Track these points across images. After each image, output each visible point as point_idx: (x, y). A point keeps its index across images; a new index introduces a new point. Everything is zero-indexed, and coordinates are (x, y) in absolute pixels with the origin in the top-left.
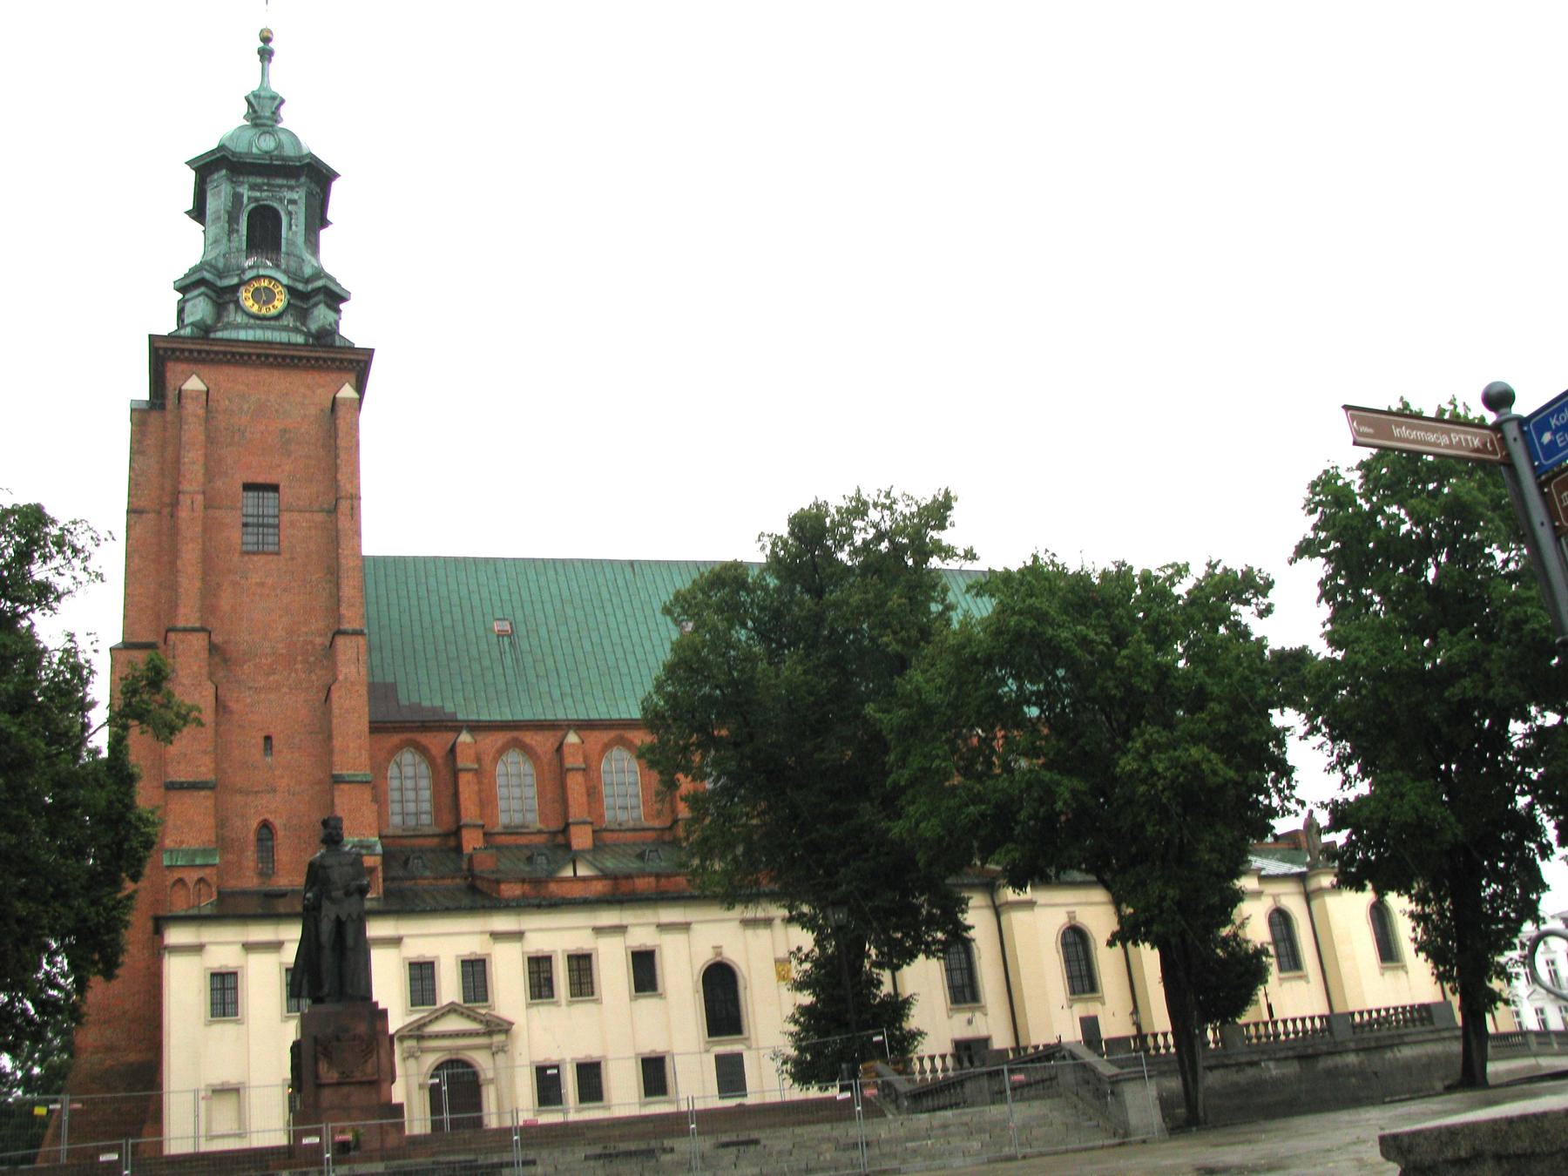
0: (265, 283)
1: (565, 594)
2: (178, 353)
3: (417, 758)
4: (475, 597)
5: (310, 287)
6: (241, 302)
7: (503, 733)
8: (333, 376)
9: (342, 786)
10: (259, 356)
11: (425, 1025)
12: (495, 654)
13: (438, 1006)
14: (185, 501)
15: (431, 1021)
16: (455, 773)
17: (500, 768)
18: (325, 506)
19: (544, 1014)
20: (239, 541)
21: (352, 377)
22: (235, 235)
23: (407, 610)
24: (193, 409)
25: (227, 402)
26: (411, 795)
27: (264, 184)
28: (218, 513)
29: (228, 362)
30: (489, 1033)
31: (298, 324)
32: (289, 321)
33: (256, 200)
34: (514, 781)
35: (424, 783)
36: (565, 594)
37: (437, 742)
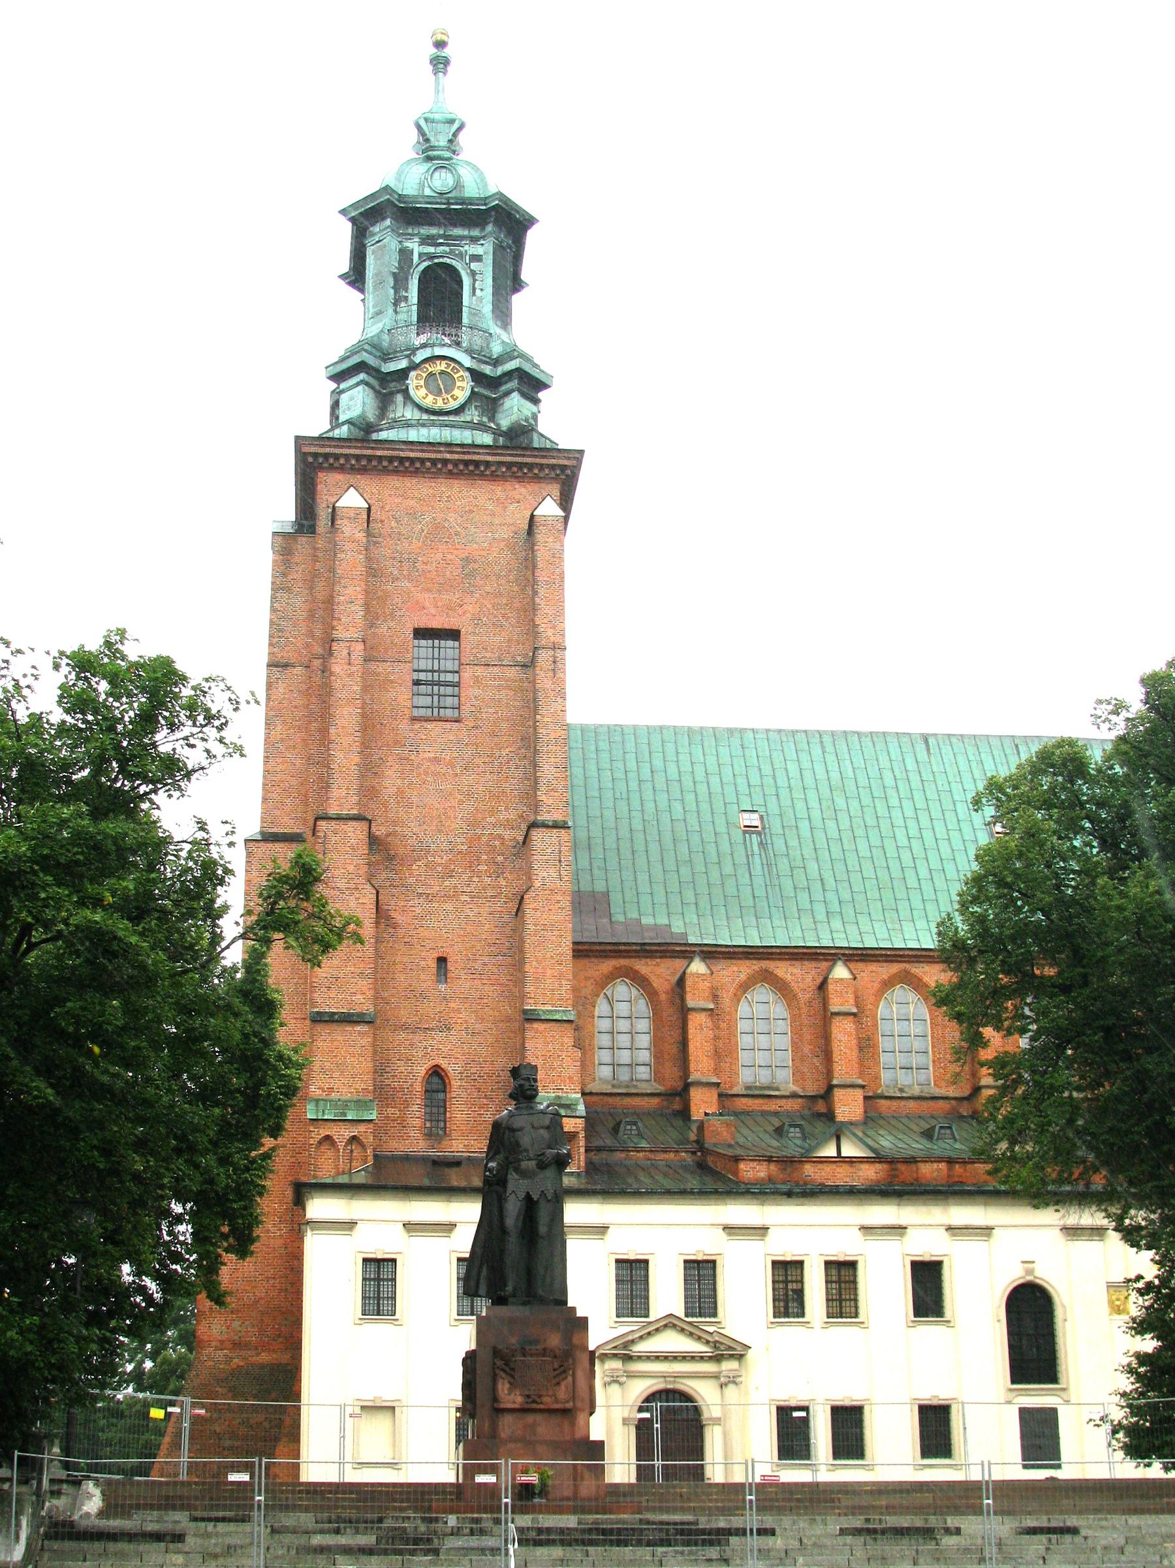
0: (441, 366)
1: (835, 776)
2: (331, 461)
3: (634, 992)
4: (715, 781)
5: (500, 371)
6: (412, 392)
7: (748, 962)
8: (533, 487)
9: (536, 1025)
10: (434, 462)
11: (633, 1342)
12: (740, 858)
13: (652, 1318)
14: (340, 650)
15: (641, 1337)
16: (684, 1012)
17: (743, 1009)
18: (519, 659)
19: (790, 1333)
20: (409, 704)
21: (555, 489)
22: (403, 304)
23: (624, 796)
24: (351, 531)
25: (393, 524)
26: (624, 1040)
27: (440, 236)
28: (381, 668)
29: (396, 472)
30: (717, 1359)
31: (485, 419)
32: (472, 415)
33: (431, 257)
34: (762, 1026)
35: (643, 1025)
36: (835, 776)
37: (661, 973)
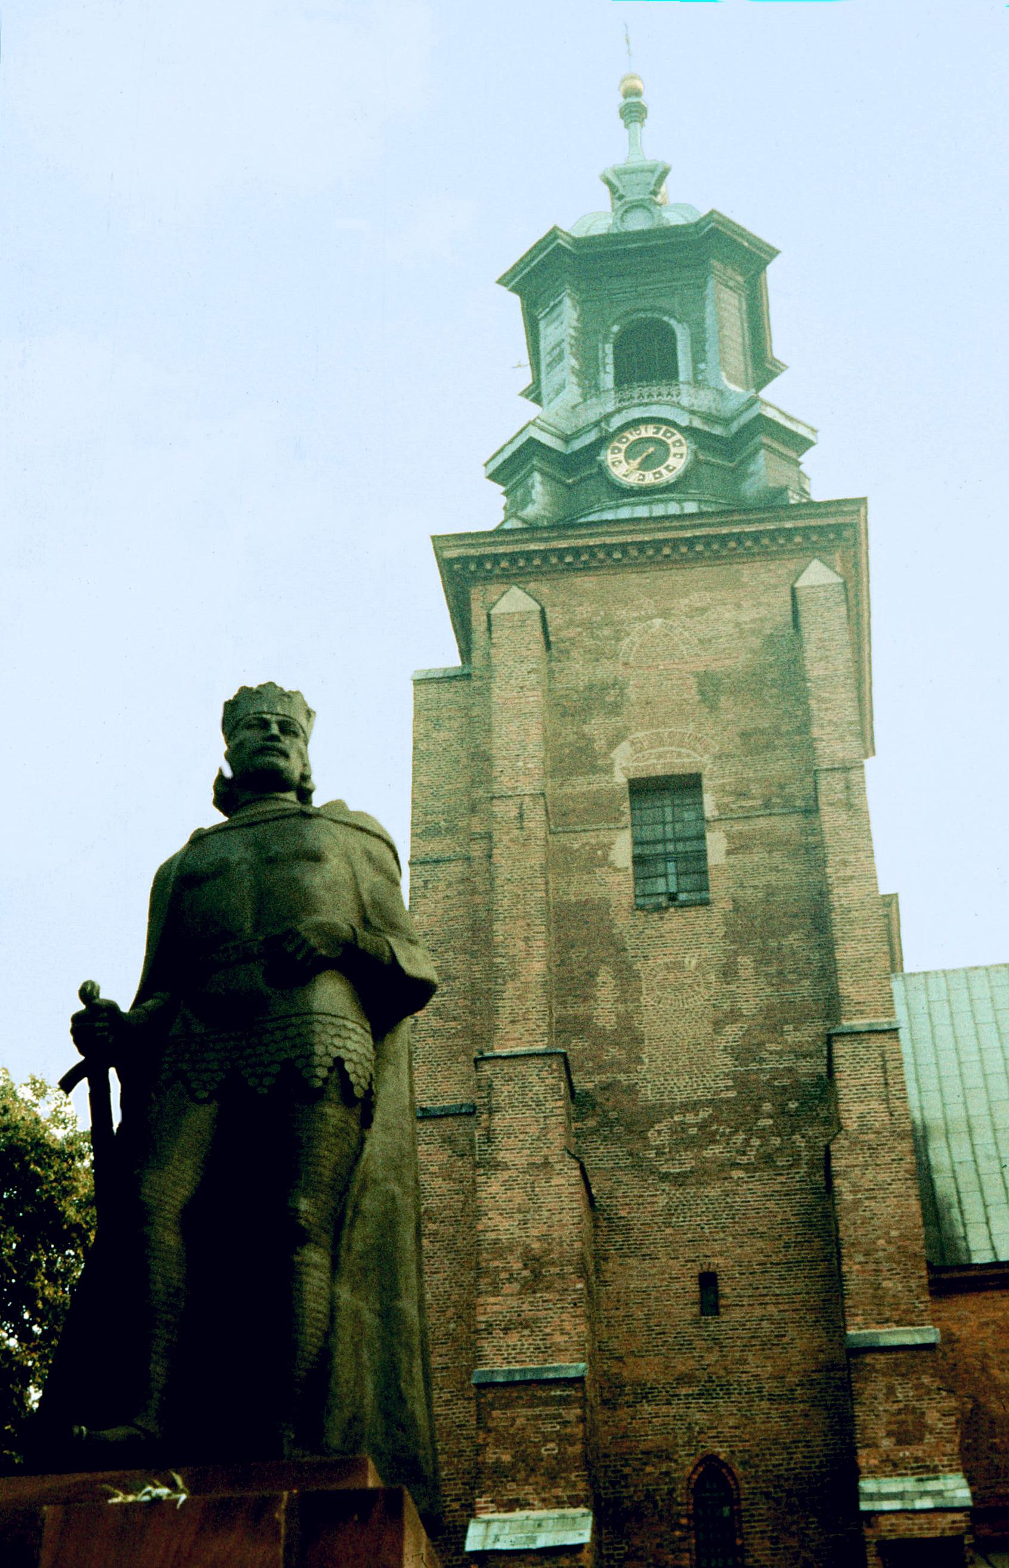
5: (735, 427)
